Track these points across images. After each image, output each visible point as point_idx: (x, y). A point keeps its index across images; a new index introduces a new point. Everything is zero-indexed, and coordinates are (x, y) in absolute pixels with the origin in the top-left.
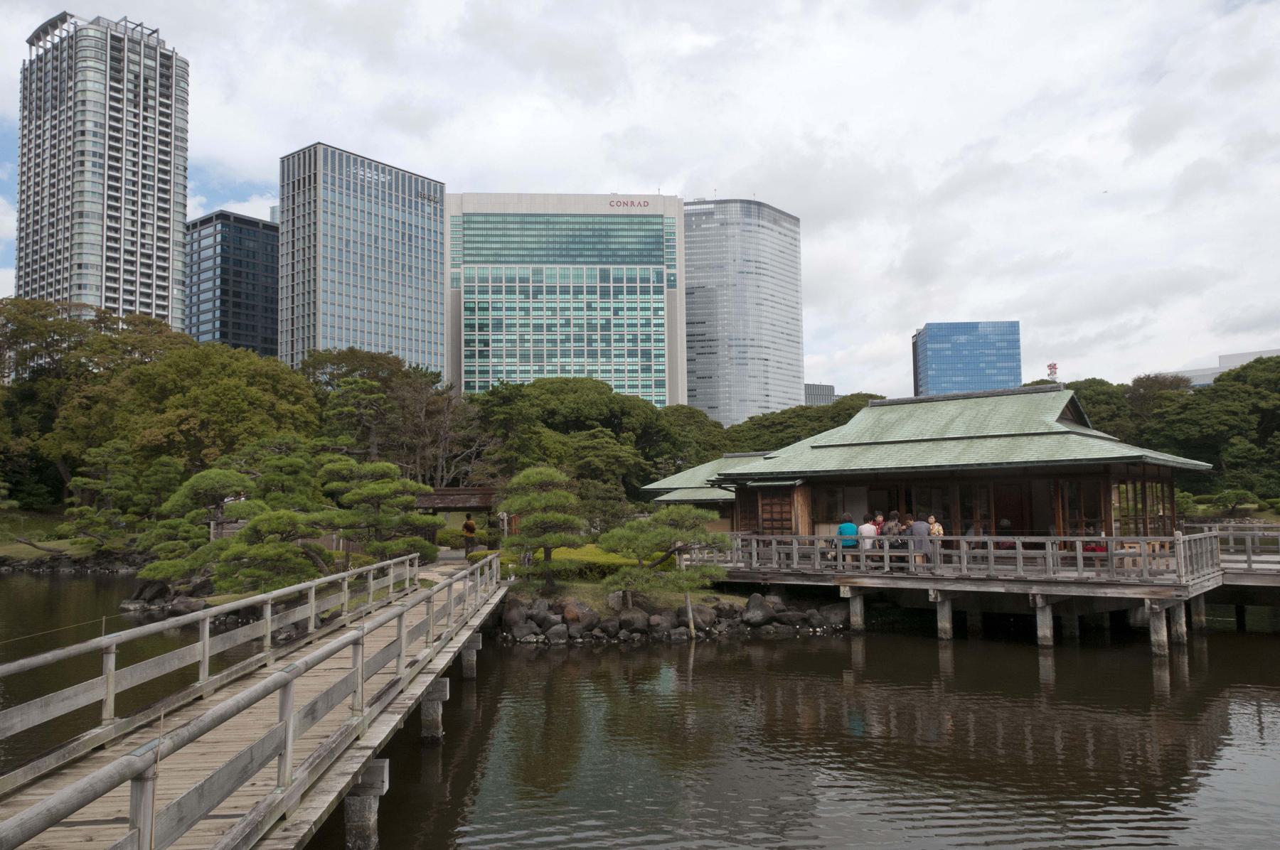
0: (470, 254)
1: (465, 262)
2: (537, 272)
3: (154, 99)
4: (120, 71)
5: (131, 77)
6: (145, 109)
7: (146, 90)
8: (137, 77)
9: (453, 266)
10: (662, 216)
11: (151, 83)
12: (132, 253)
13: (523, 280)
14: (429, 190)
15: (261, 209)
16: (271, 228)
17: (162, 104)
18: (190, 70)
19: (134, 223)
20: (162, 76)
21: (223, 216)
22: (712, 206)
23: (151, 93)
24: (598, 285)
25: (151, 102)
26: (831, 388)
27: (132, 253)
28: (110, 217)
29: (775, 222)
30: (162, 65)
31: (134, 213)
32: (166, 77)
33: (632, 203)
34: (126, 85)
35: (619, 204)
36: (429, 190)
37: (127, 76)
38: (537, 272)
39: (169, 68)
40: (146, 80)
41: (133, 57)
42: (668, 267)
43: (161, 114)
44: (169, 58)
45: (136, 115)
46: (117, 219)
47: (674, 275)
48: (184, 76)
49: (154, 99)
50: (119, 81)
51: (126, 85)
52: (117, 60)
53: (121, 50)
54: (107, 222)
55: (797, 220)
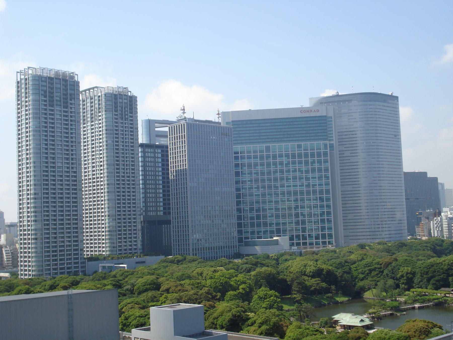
2: (268, 149)
6: (125, 120)
8: (122, 108)
10: (326, 116)
11: (126, 109)
13: (261, 151)
18: (138, 99)
23: (126, 113)
25: (126, 117)
26: (425, 173)
32: (131, 105)
33: (311, 111)
35: (305, 111)
37: (119, 108)
40: (125, 108)
41: (121, 100)
42: (330, 140)
47: (333, 144)
50: (116, 111)
51: (119, 112)
52: (116, 103)
55: (397, 98)
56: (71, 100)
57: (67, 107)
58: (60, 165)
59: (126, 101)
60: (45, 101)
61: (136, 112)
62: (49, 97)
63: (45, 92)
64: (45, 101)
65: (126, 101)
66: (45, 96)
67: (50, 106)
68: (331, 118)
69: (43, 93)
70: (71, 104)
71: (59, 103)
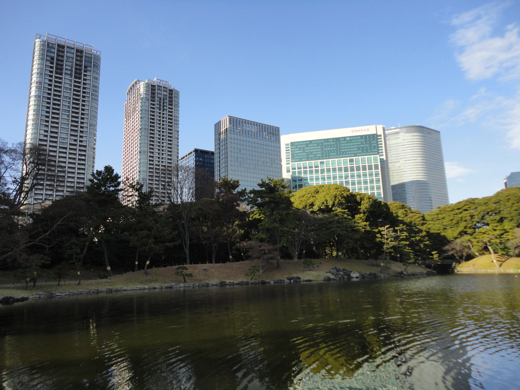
0: (295, 157)
1: (292, 162)
3: (166, 106)
4: (154, 97)
5: (158, 99)
6: (163, 111)
7: (163, 103)
8: (160, 99)
9: (287, 164)
11: (165, 101)
12: (158, 165)
14: (273, 131)
15: (209, 146)
16: (213, 153)
17: (169, 108)
19: (159, 154)
20: (169, 97)
21: (196, 151)
22: (398, 130)
23: (165, 104)
24: (349, 166)
25: (165, 108)
27: (158, 165)
28: (150, 152)
29: (429, 133)
30: (169, 94)
31: (159, 150)
32: (171, 98)
34: (156, 103)
36: (273, 131)
38: (322, 163)
39: (172, 94)
40: (163, 100)
41: (159, 92)
42: (380, 156)
43: (169, 112)
44: (171, 91)
45: (160, 113)
46: (153, 153)
48: (178, 98)
49: (166, 106)
50: (154, 101)
52: (153, 94)
53: (154, 90)
54: (150, 154)
55: (439, 132)
56: (85, 71)
57: (80, 78)
58: (64, 136)
59: (165, 93)
60: (52, 67)
61: (177, 106)
62: (57, 64)
63: (52, 58)
64: (52, 67)
65: (165, 93)
66: (52, 63)
67: (56, 73)
68: (381, 136)
69: (49, 58)
70: (85, 75)
71: (69, 72)
